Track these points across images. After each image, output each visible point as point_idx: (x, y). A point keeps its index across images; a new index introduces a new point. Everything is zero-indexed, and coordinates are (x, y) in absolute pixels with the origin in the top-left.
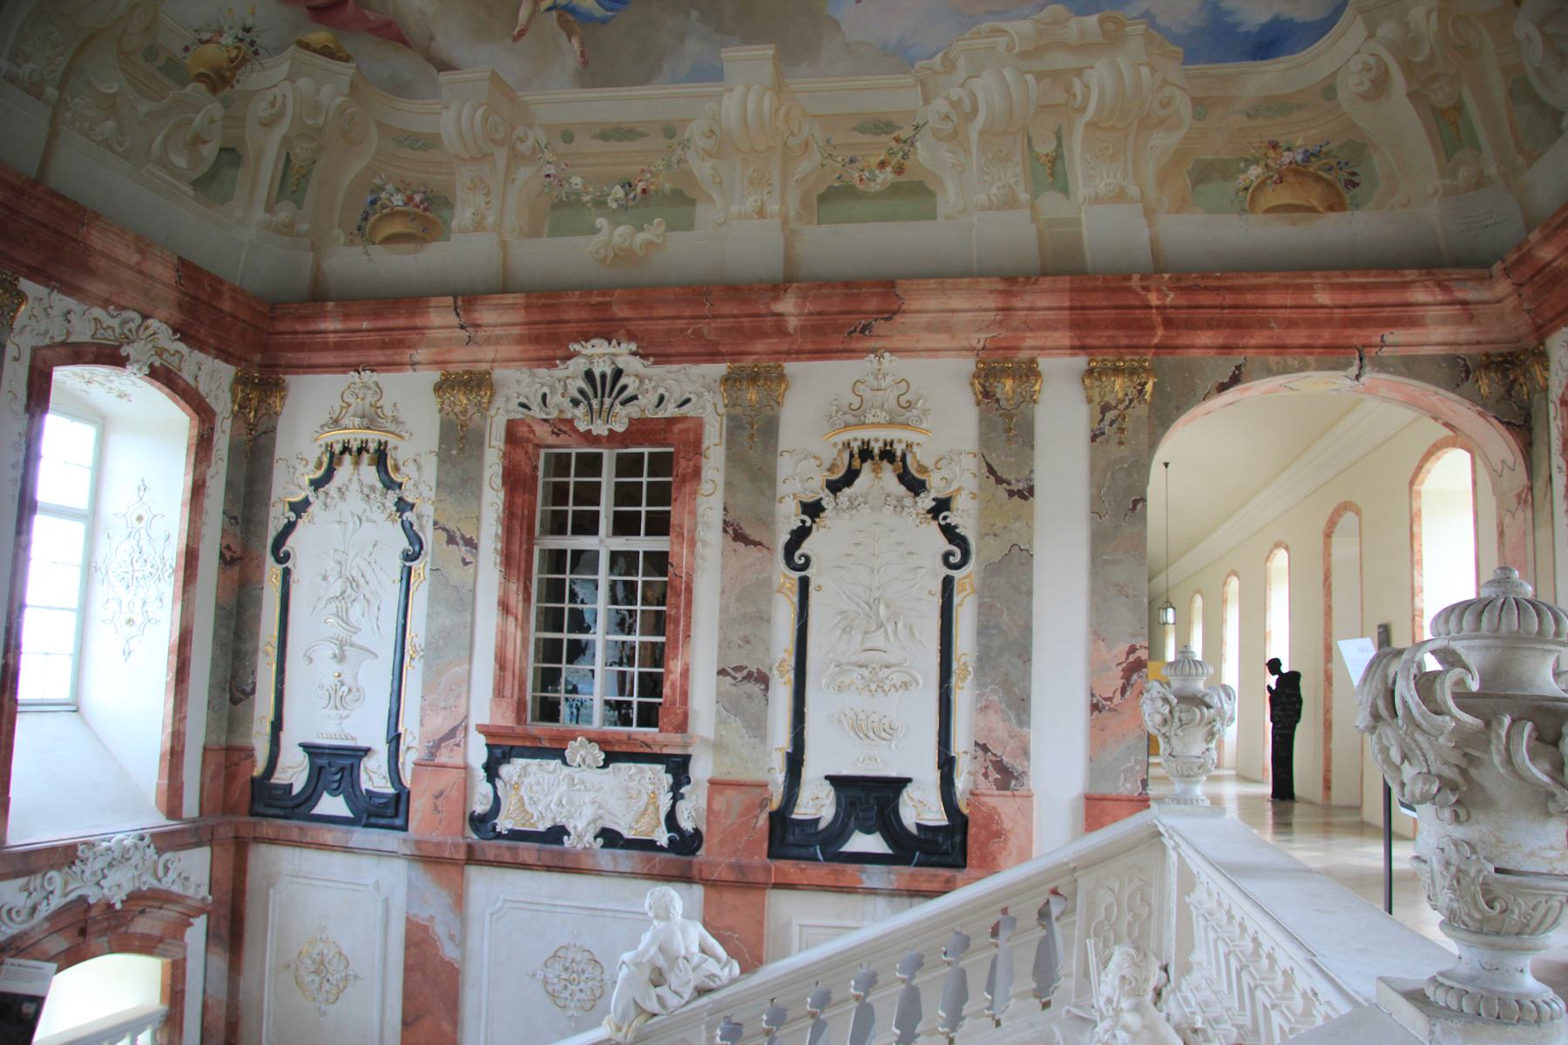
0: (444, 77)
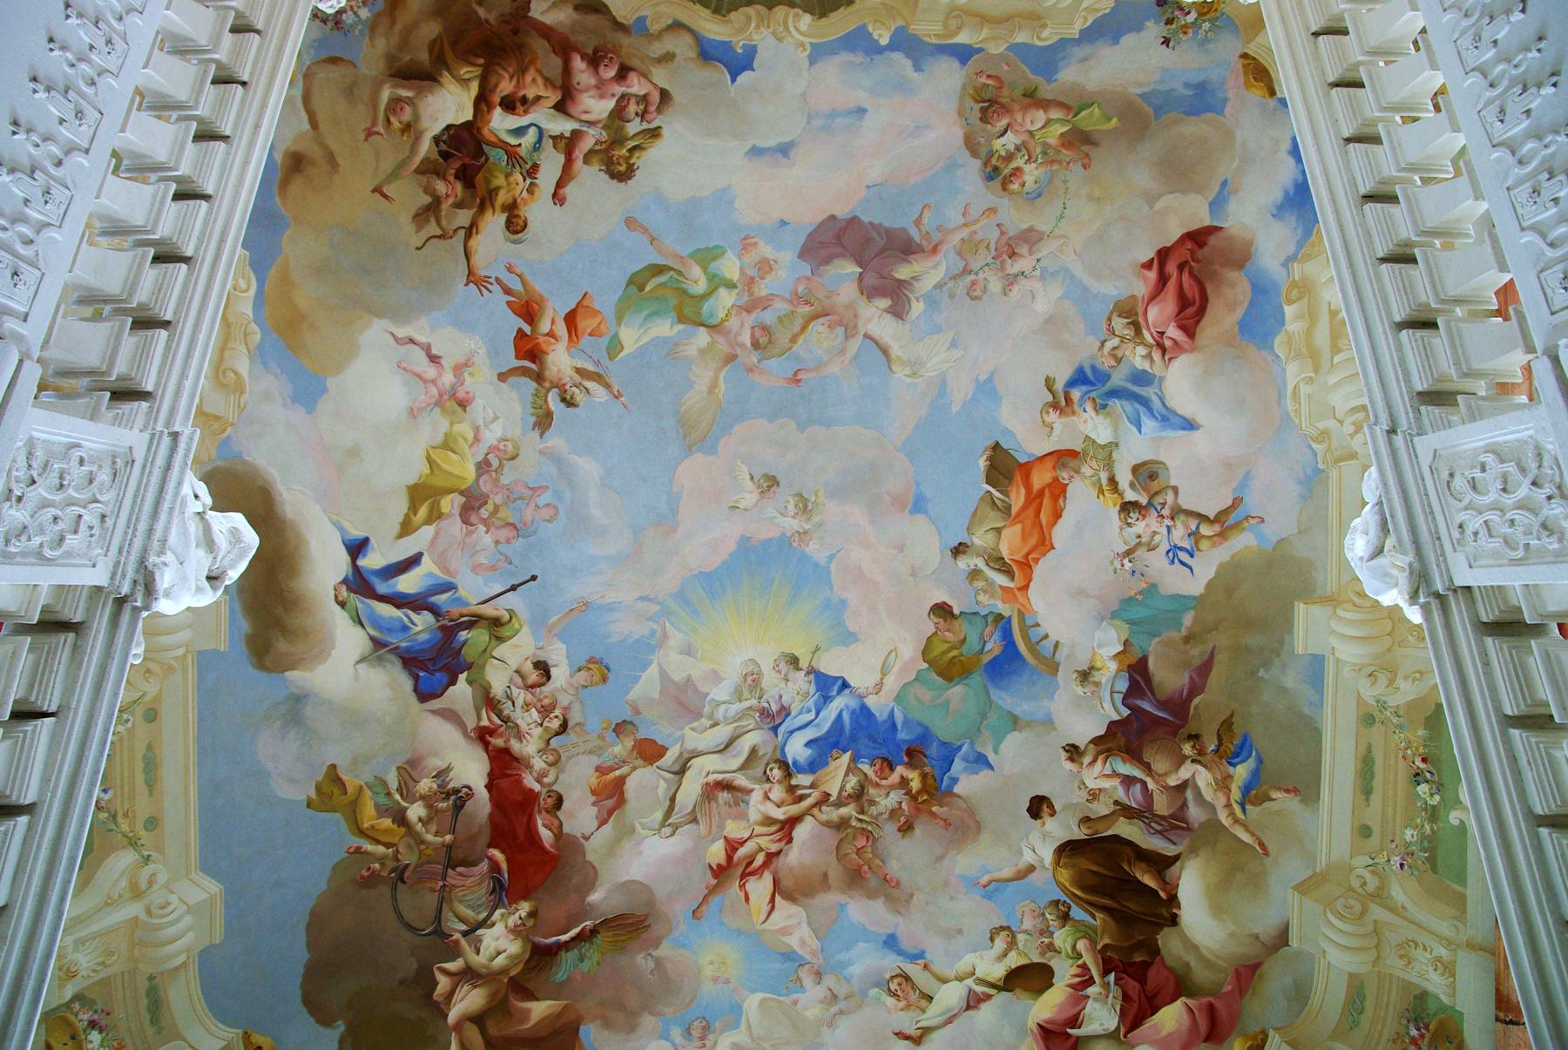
0: (1294, 942)
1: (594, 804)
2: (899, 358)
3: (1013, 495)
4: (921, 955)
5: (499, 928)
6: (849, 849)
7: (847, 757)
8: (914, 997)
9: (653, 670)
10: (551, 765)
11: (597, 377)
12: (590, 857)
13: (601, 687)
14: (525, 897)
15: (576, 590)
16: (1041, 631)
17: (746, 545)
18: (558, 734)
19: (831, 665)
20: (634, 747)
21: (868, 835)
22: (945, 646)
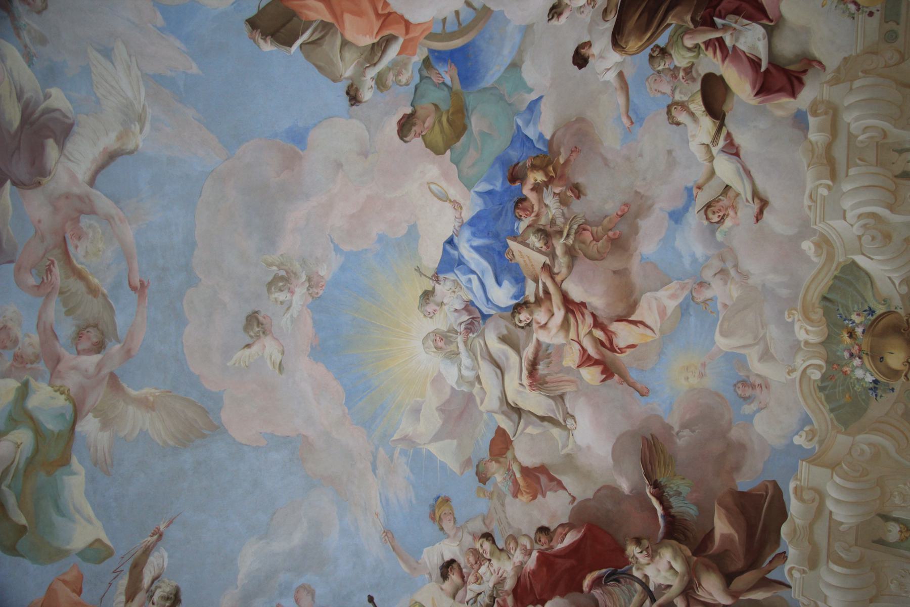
1: (544, 496)
2: (120, 138)
3: (312, 15)
4: (689, 190)
5: (650, 571)
6: (594, 248)
7: (512, 244)
8: (725, 201)
9: (433, 448)
10: (517, 543)
11: (137, 568)
12: (590, 494)
13: (454, 503)
14: (623, 550)
15: (374, 547)
16: (451, 18)
17: (320, 351)
18: (494, 542)
19: (432, 256)
20: (498, 462)
21: (581, 229)
22: (437, 128)
